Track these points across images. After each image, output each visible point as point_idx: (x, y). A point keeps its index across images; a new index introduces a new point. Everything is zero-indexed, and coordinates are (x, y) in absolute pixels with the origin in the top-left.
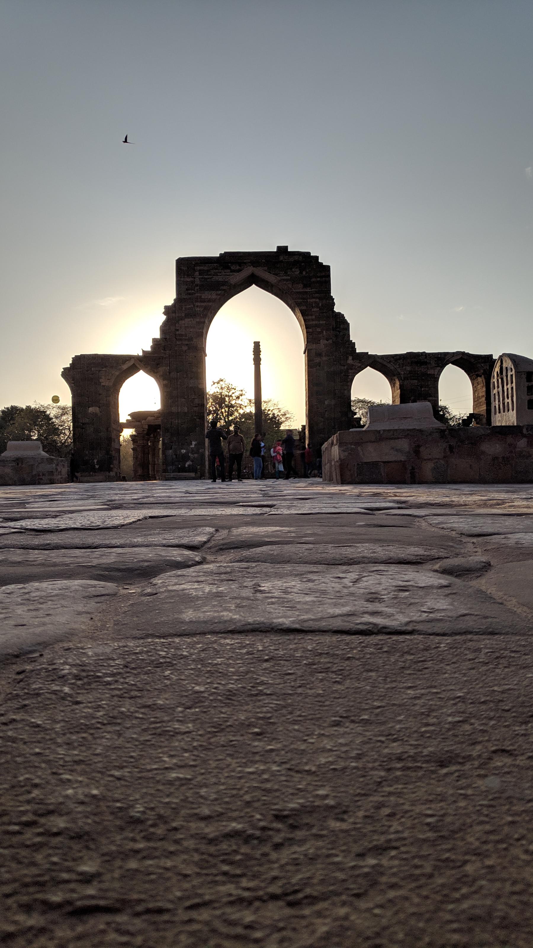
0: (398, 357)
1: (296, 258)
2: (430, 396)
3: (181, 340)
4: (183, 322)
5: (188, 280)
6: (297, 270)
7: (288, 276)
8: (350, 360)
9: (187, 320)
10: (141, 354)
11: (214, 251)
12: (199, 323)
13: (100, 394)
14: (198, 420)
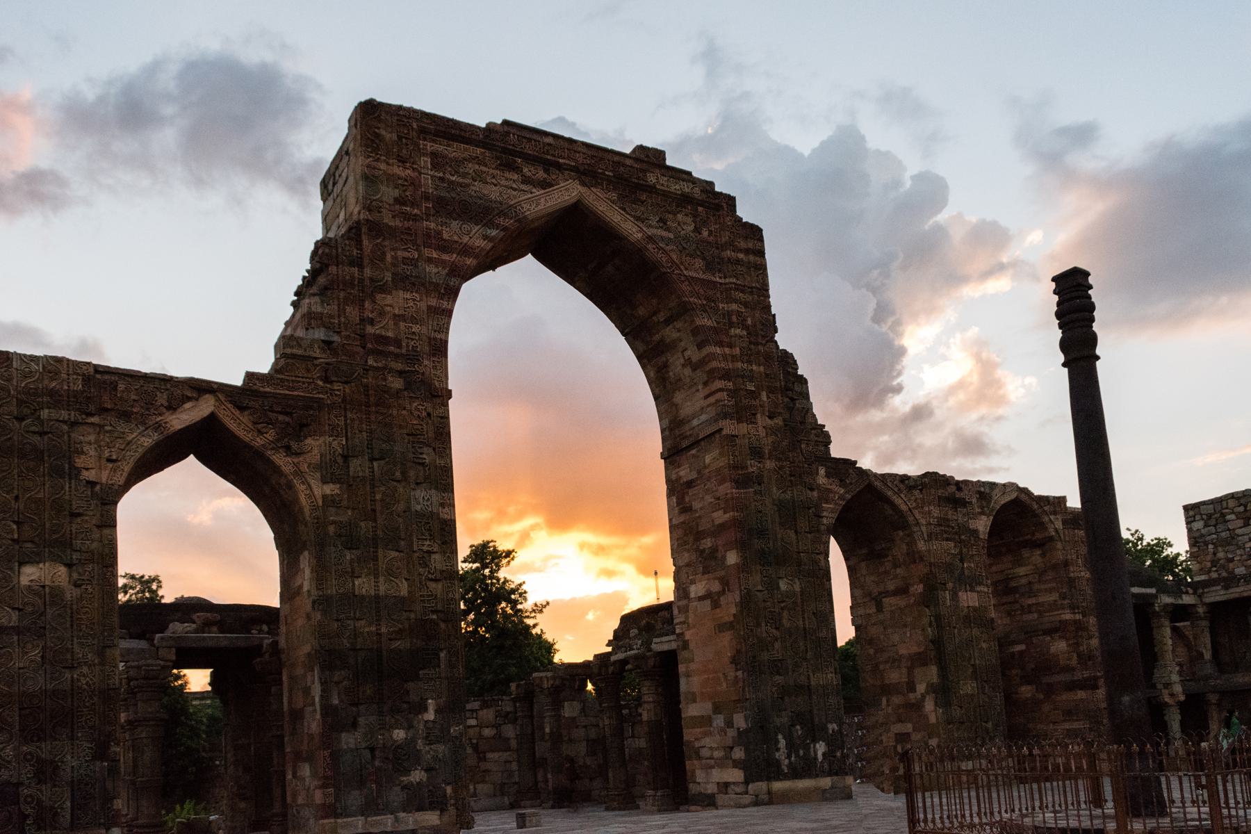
0: (912, 483)
2: (980, 584)
3: (380, 353)
4: (389, 299)
6: (689, 220)
7: (668, 230)
8: (822, 479)
10: (238, 381)
13: (74, 515)
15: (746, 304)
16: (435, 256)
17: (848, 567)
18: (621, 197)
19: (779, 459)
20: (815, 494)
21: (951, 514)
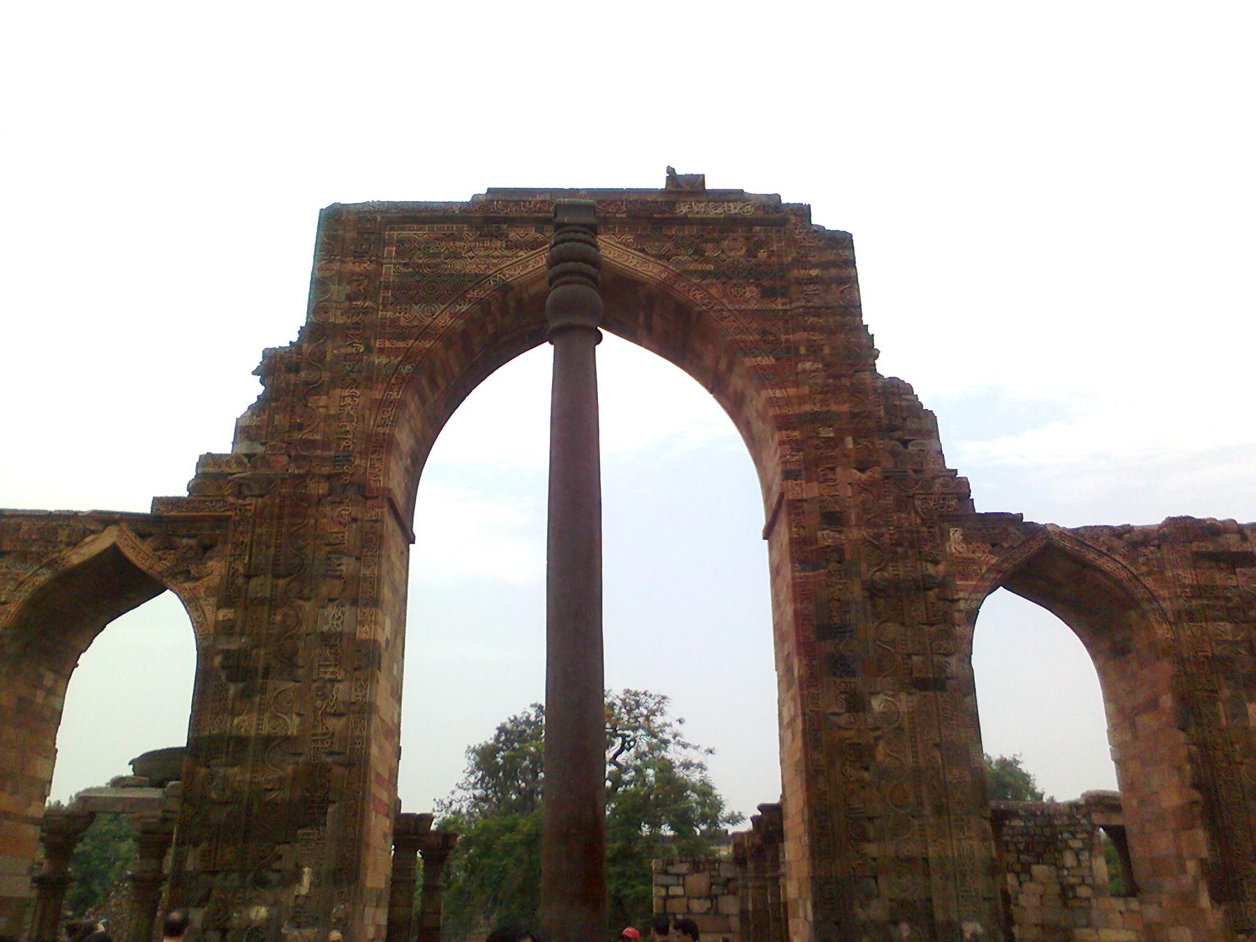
1: (734, 209)
4: (323, 400)
5: (358, 269)
9: (337, 392)
11: (457, 188)
12: (380, 405)
14: (337, 771)
15: (822, 330)
16: (387, 344)
17: (1099, 669)
18: (638, 238)
19: (876, 525)
20: (941, 568)
21: (1220, 578)
